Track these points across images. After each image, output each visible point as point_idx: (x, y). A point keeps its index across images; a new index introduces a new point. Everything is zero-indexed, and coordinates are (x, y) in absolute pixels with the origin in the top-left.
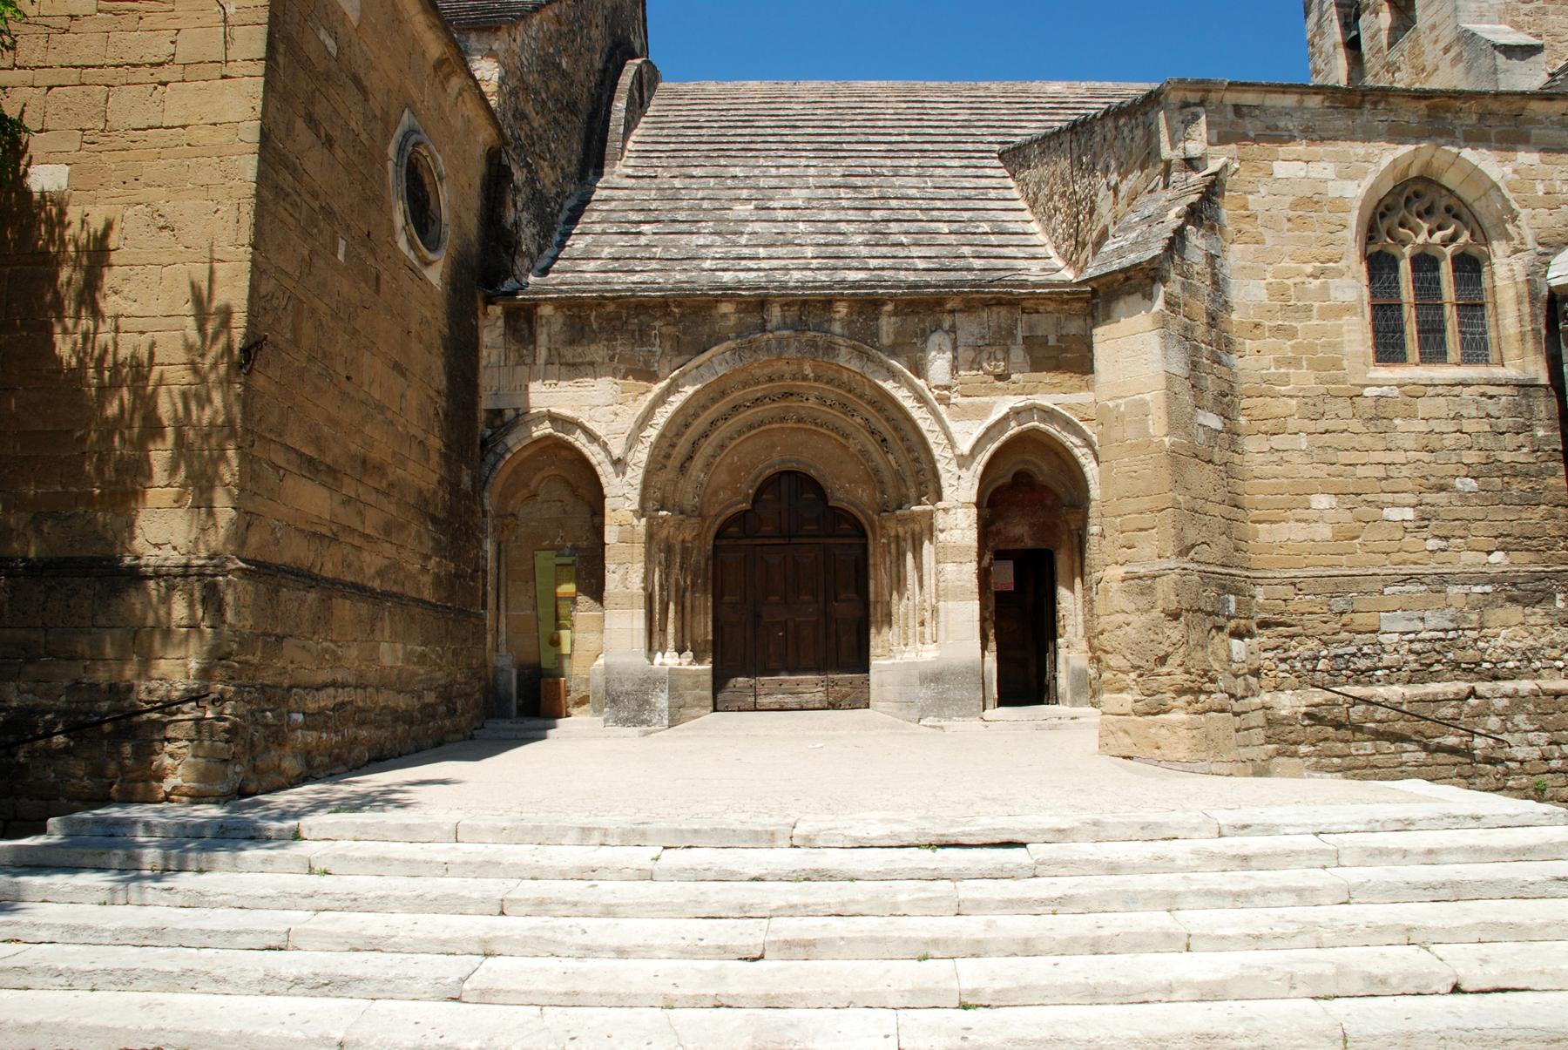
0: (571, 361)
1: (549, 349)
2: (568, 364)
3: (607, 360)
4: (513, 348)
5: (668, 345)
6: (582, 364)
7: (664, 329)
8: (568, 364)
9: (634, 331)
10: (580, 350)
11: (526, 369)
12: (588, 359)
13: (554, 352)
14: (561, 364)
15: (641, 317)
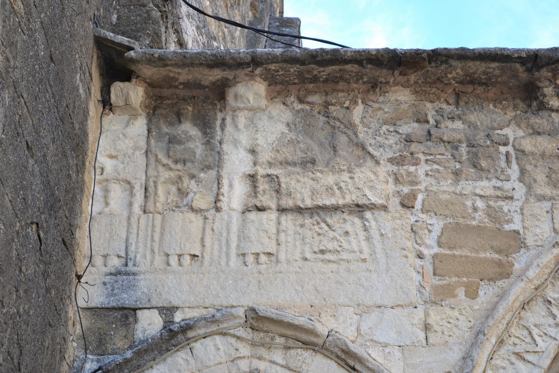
0: (309, 203)
1: (252, 178)
2: (299, 210)
3: (394, 203)
4: (165, 174)
5: (541, 177)
6: (336, 209)
7: (528, 145)
8: (299, 210)
9: (454, 145)
10: (330, 179)
11: (196, 221)
12: (348, 199)
13: (263, 185)
14: (282, 210)
15: (473, 117)
